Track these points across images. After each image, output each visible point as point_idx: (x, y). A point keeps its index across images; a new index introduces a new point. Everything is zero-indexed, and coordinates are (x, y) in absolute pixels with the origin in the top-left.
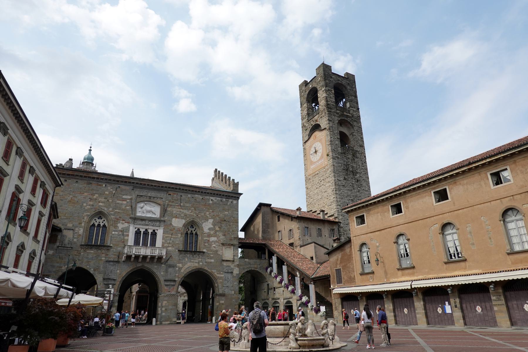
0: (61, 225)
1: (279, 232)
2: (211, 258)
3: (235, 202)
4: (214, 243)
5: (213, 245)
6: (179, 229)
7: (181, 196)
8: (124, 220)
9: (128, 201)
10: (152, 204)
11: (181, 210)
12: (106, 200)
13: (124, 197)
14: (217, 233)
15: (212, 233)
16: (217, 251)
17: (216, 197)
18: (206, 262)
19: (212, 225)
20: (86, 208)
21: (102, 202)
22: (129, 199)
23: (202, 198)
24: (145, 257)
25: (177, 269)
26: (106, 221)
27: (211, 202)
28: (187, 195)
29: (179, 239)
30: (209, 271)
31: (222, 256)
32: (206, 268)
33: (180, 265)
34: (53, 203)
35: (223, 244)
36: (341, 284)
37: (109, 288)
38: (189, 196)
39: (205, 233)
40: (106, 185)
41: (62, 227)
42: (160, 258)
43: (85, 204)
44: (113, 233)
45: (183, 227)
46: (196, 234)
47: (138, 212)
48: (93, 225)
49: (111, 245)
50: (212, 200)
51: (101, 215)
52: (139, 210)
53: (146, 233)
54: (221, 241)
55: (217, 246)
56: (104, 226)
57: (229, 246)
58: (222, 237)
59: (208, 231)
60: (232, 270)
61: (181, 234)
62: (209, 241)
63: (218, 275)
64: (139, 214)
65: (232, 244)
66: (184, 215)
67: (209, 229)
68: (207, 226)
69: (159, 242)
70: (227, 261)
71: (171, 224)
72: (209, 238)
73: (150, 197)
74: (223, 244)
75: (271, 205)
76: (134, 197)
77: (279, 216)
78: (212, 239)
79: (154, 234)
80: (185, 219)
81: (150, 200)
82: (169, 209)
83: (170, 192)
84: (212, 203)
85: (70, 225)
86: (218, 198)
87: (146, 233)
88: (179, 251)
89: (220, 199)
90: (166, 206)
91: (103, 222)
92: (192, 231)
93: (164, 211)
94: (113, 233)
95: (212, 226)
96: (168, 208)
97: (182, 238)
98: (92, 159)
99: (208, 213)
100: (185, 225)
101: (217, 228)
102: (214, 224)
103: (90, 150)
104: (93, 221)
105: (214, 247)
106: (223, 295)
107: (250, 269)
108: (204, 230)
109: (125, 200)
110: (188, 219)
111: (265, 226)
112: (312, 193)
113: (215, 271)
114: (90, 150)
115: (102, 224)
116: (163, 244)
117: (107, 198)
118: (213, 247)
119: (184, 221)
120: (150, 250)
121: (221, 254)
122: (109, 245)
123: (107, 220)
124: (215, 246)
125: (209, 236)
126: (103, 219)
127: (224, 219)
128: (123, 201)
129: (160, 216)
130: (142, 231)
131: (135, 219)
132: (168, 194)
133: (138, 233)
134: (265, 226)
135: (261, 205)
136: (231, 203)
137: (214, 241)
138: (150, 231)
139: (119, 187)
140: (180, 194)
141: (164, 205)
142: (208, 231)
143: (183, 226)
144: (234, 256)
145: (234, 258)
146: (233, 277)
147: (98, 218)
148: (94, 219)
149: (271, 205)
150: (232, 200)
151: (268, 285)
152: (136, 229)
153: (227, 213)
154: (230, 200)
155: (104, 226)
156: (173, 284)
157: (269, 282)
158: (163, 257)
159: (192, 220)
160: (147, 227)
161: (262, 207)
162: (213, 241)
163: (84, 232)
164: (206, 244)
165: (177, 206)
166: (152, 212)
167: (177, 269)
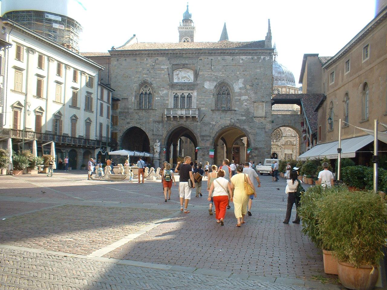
0: (119, 96)
2: (242, 116)
3: (267, 58)
4: (245, 102)
5: (244, 104)
6: (212, 91)
7: (212, 59)
8: (164, 87)
9: (165, 70)
10: (188, 70)
11: (213, 73)
12: (148, 72)
13: (162, 67)
14: (248, 91)
15: (243, 91)
16: (248, 109)
17: (246, 56)
18: (237, 119)
19: (243, 84)
20: (135, 80)
21: (145, 74)
22: (166, 69)
23: (232, 59)
24: (181, 117)
25: (211, 126)
26: (151, 89)
27: (241, 62)
28: (217, 58)
29: (211, 100)
30: (242, 127)
31: (253, 113)
32: (238, 125)
33: (214, 123)
34: (99, 83)
36: (321, 141)
37: (156, 142)
38: (219, 58)
39: (236, 93)
40: (147, 59)
41: (120, 99)
42: (194, 117)
43: (133, 78)
44: (156, 98)
45: (215, 89)
46: (228, 94)
47: (174, 79)
48: (142, 93)
49: (156, 109)
50: (242, 59)
51: (147, 85)
52: (175, 77)
53: (183, 97)
55: (248, 104)
56: (150, 94)
58: (253, 95)
59: (239, 90)
61: (214, 95)
62: (240, 99)
63: (250, 131)
64: (175, 81)
66: (215, 78)
67: (240, 89)
68: (238, 86)
69: (194, 105)
71: (203, 87)
72: (239, 97)
73: (184, 65)
75: (318, 55)
76: (170, 66)
78: (243, 98)
79: (190, 97)
80: (216, 81)
81: (184, 66)
82: (200, 73)
83: (201, 58)
84: (242, 62)
85: (125, 96)
86: (248, 57)
87: (183, 97)
88: (212, 110)
89: (251, 57)
90: (198, 71)
91: (149, 90)
92: (224, 91)
93: (196, 75)
94: (156, 98)
95: (243, 86)
96: (199, 73)
97: (214, 99)
98: (190, 16)
99: (238, 73)
100: (215, 87)
101: (248, 87)
102: (245, 83)
103: (188, 6)
104: (141, 90)
106: (256, 149)
108: (235, 90)
109: (163, 69)
110: (219, 81)
111: (311, 79)
113: (247, 127)
114: (188, 6)
115: (148, 92)
116: (197, 105)
117: (149, 70)
119: (215, 84)
120: (184, 111)
121: (252, 111)
122: (154, 109)
123: (152, 89)
124: (246, 104)
125: (240, 95)
126: (148, 88)
127: (255, 77)
128: (161, 71)
129: (194, 81)
130: (179, 95)
131: (173, 86)
132: (199, 59)
133: (176, 97)
135: (306, 56)
136: (263, 60)
137: (246, 100)
138: (186, 95)
139: (157, 59)
140: (210, 58)
141: (196, 71)
142: (239, 90)
143: (214, 88)
145: (266, 114)
146: (266, 132)
147: (145, 87)
148: (142, 89)
149: (318, 55)
150: (264, 57)
152: (175, 94)
153: (259, 70)
154: (262, 57)
155: (150, 94)
156: (208, 138)
158: (195, 117)
159: (222, 81)
160: (182, 92)
161: (308, 58)
162: (244, 100)
163: (135, 99)
164: (238, 103)
165: (208, 69)
166: (187, 78)
167: (211, 126)
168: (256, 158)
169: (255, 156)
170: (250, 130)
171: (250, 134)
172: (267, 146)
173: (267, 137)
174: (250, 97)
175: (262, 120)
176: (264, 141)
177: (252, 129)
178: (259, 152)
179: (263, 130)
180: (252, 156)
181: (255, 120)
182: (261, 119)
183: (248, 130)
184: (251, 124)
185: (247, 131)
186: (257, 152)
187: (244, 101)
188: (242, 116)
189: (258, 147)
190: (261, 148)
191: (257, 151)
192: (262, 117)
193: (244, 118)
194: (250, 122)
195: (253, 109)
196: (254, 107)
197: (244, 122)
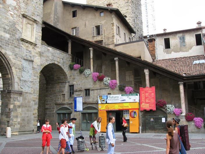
1: (73, 28)
5: (9, 12)
16: (14, 24)
31: (21, 33)
35: (24, 16)
54: (22, 10)
55: (15, 16)
57: (31, 22)
60: (32, 59)
65: (35, 20)
70: (27, 42)
74: (24, 16)
77: (76, 11)
105: (11, 14)
106: (20, 93)
107: (53, 62)
112: (96, 3)
113: (11, 53)
118: (9, 15)
121: (20, 30)
124: (13, 13)
134: (56, 19)
144: (36, 38)
146: (34, 68)
151: (72, 87)
157: (74, 83)
168: (19, 110)
169: (19, 107)
170: (14, 60)
171: (14, 67)
172: (34, 91)
173: (35, 76)
174: (19, 6)
175: (31, 48)
176: (31, 82)
177: (18, 58)
178: (25, 99)
179: (31, 63)
180: (15, 106)
181: (22, 45)
182: (30, 45)
183: (12, 59)
184: (17, 50)
185: (10, 59)
186: (21, 98)
187: (10, 7)
188: (4, 32)
189: (23, 90)
190: (27, 93)
191: (21, 98)
192: (31, 43)
193: (7, 36)
194: (16, 47)
195: (22, 26)
196: (22, 22)
197: (7, 43)
